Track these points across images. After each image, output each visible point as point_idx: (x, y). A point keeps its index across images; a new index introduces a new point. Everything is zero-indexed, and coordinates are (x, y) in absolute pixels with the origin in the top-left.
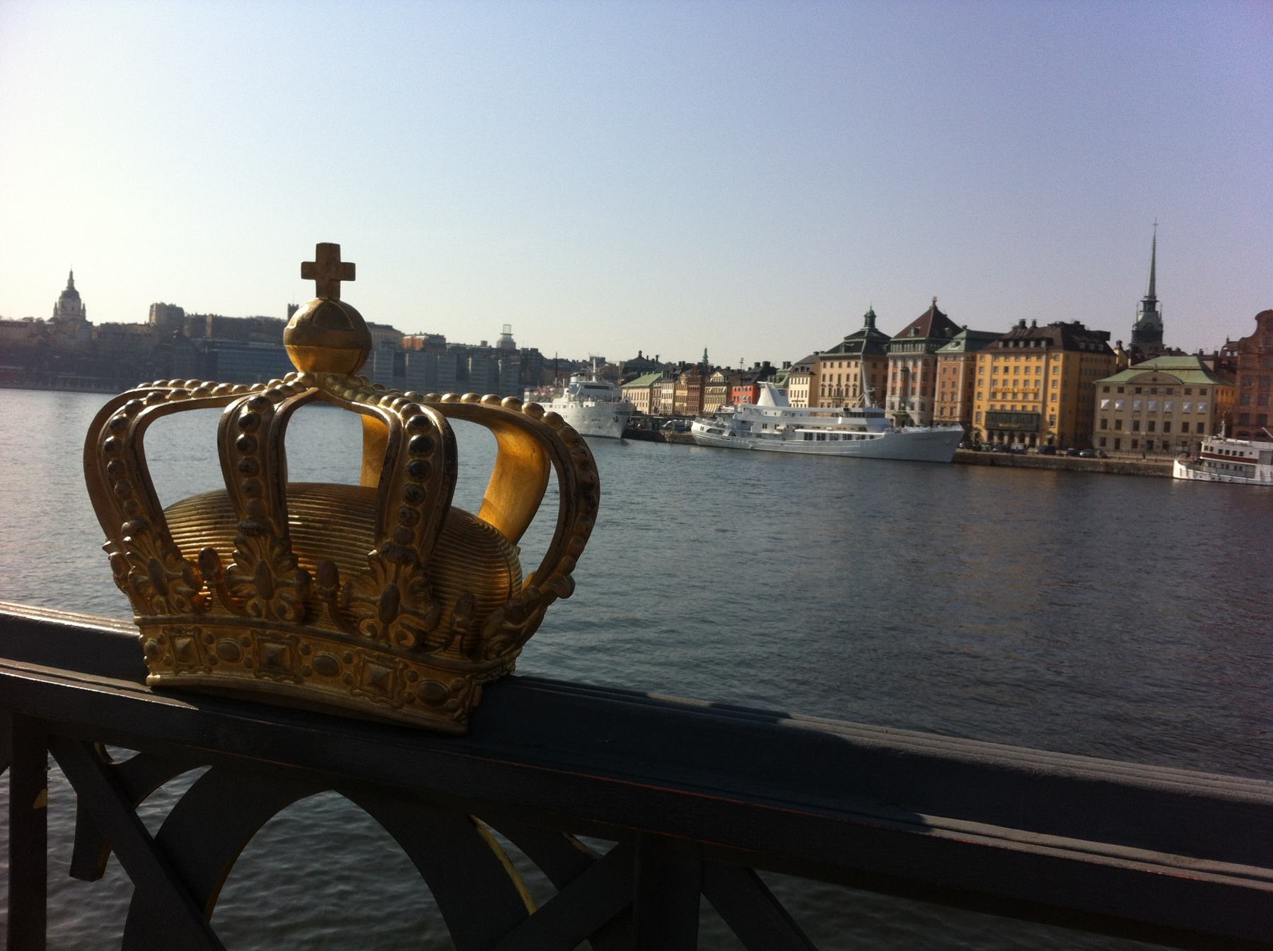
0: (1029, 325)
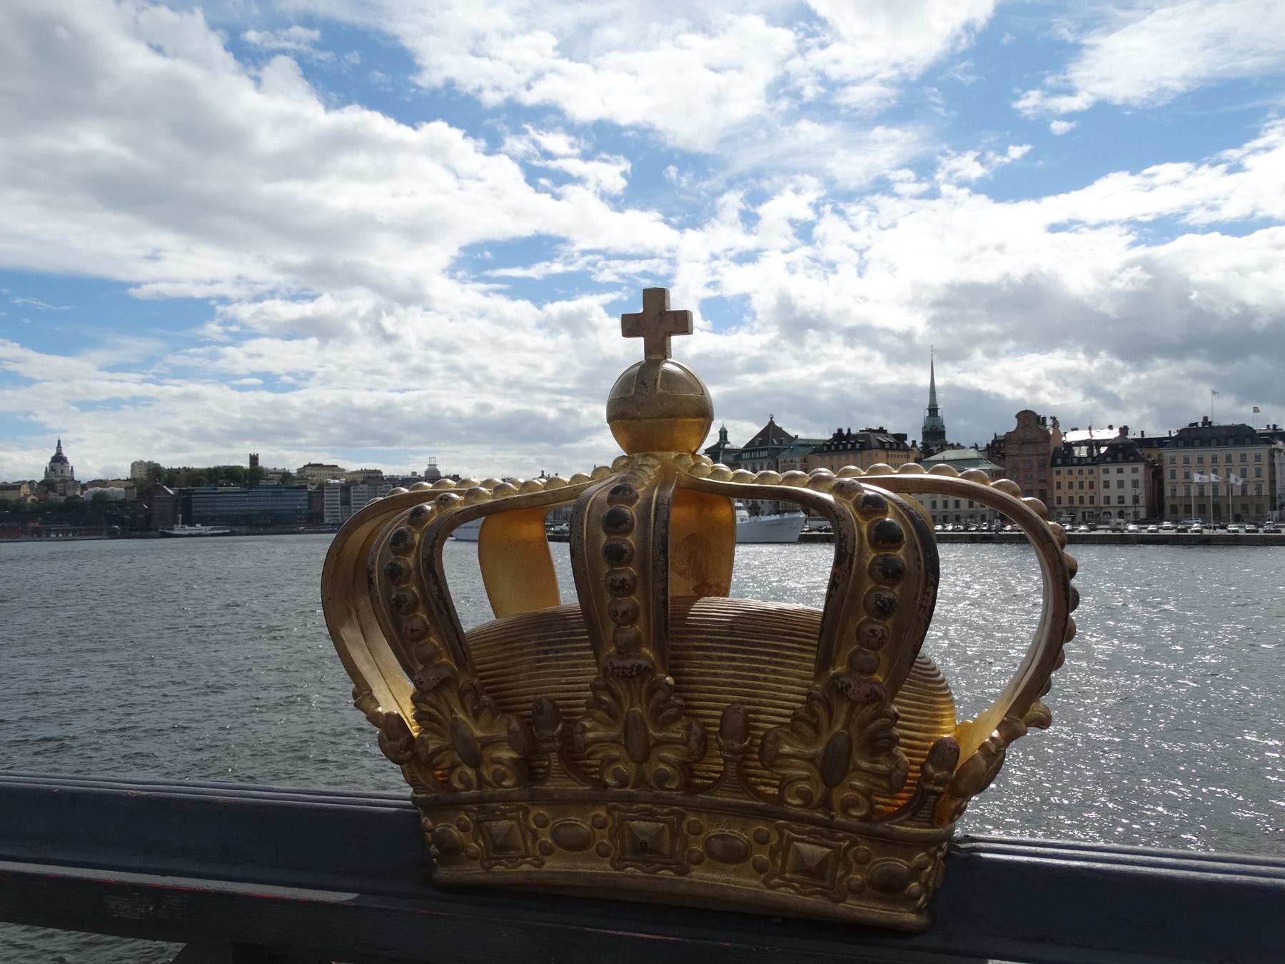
0: (845, 432)
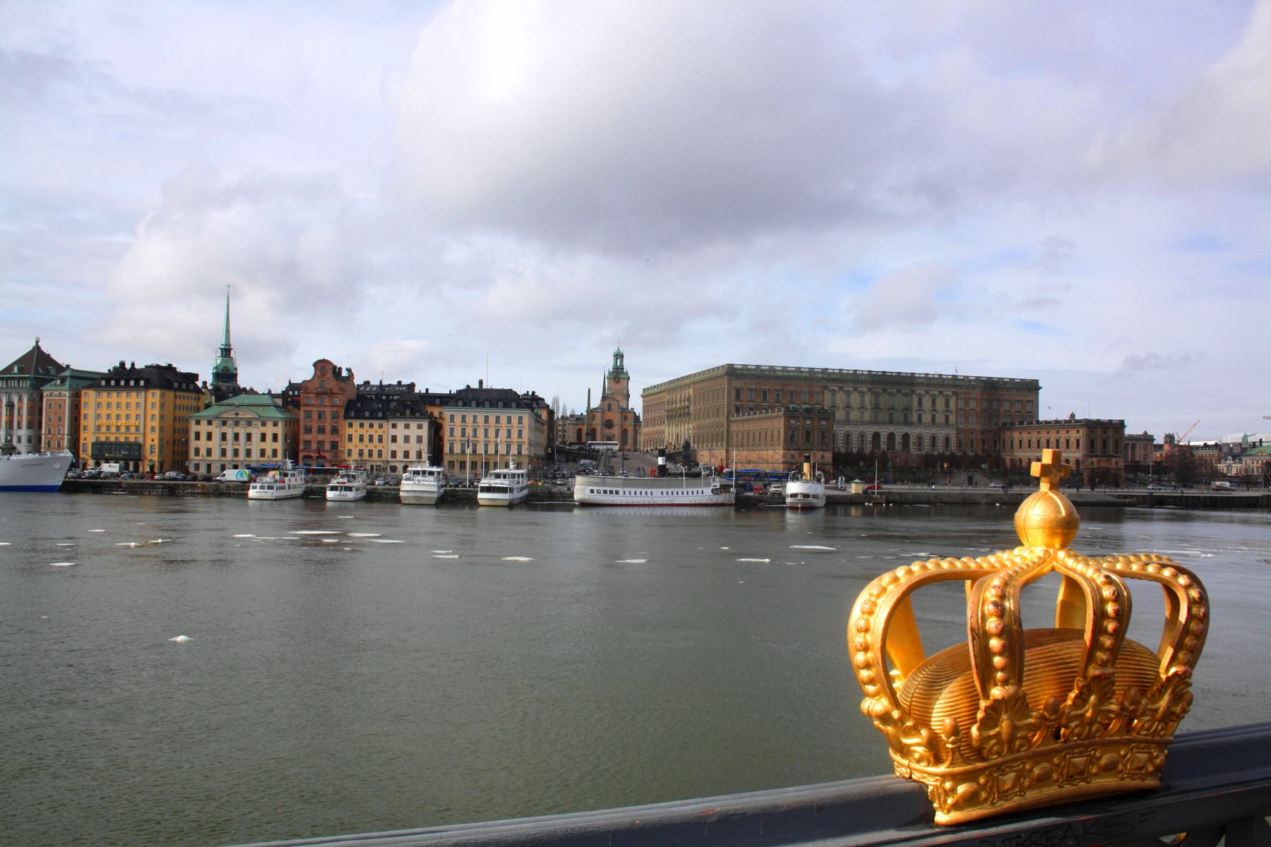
0: (128, 366)
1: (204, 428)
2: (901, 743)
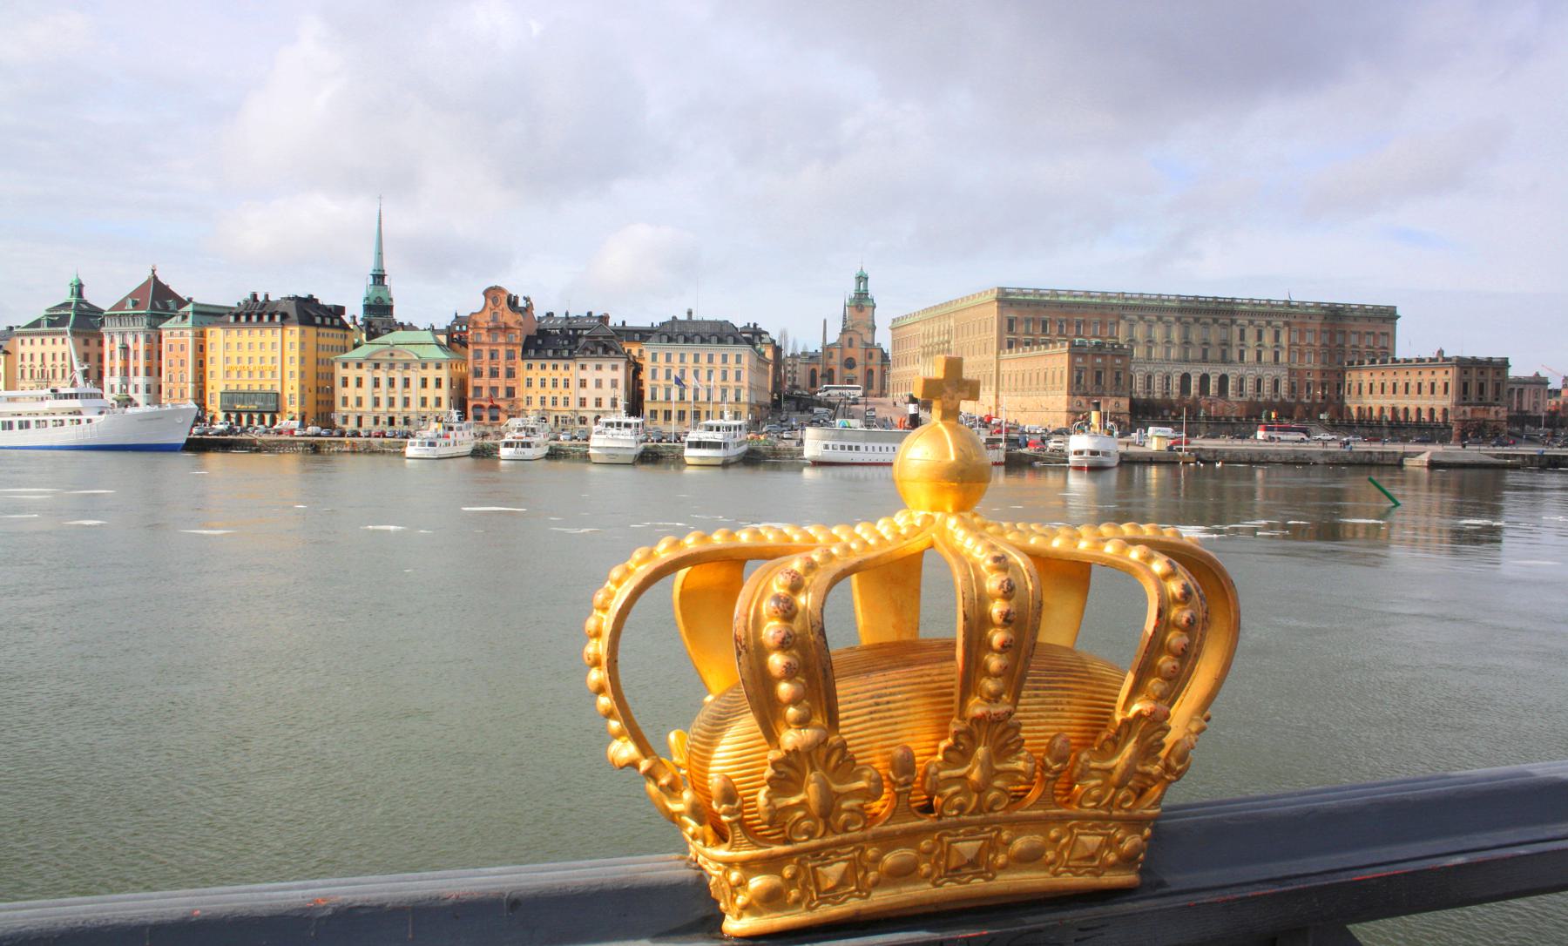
1: (352, 373)
2: (667, 809)
